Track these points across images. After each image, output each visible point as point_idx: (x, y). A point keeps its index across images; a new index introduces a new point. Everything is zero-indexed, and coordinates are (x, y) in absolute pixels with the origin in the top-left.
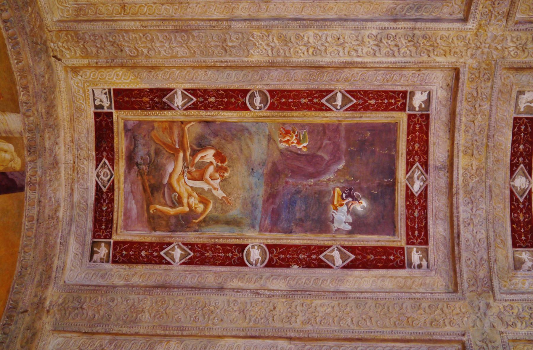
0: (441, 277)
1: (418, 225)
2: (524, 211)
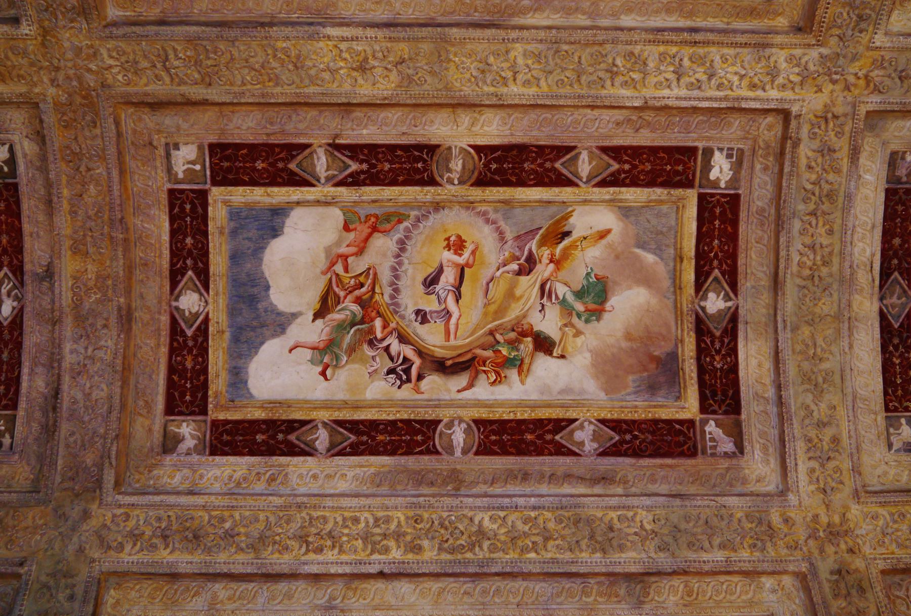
0: (28, 464)
1: (6, 375)
2: (194, 352)
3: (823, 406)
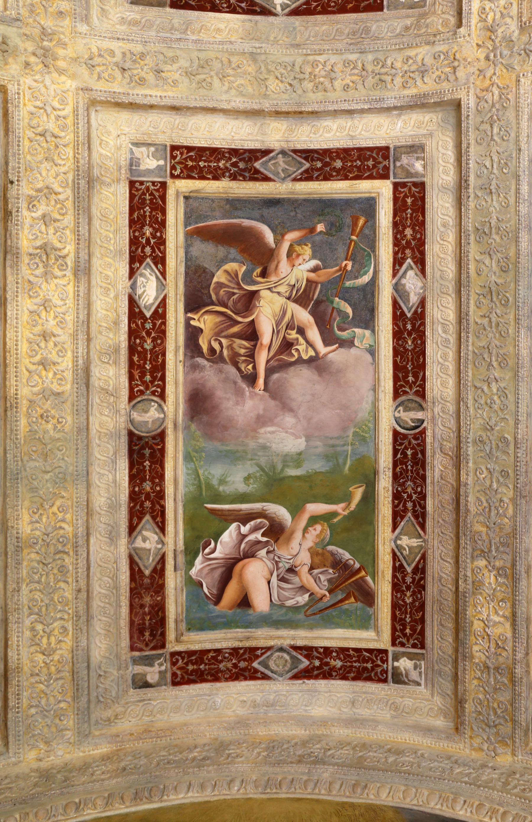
3: (177, 76)
